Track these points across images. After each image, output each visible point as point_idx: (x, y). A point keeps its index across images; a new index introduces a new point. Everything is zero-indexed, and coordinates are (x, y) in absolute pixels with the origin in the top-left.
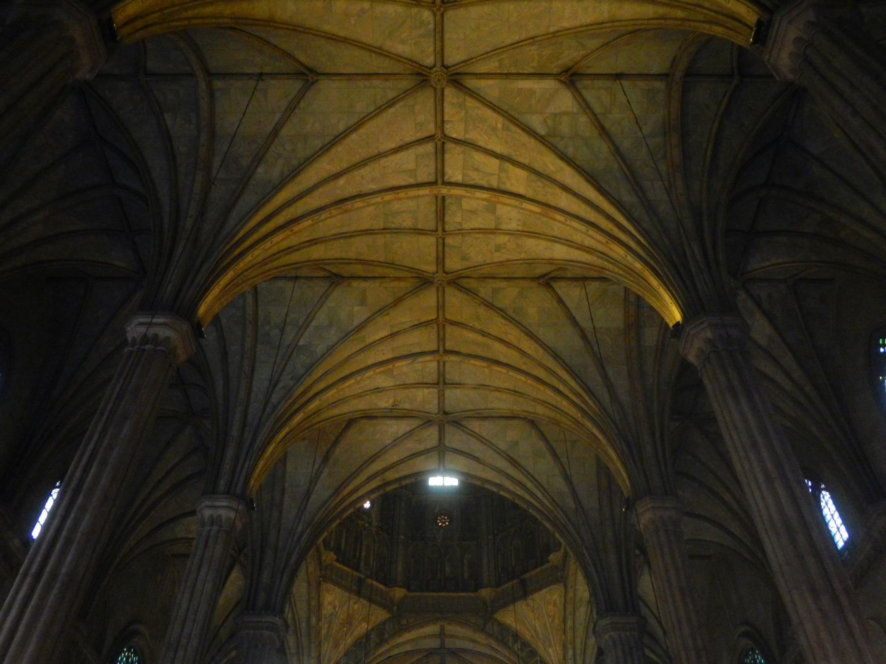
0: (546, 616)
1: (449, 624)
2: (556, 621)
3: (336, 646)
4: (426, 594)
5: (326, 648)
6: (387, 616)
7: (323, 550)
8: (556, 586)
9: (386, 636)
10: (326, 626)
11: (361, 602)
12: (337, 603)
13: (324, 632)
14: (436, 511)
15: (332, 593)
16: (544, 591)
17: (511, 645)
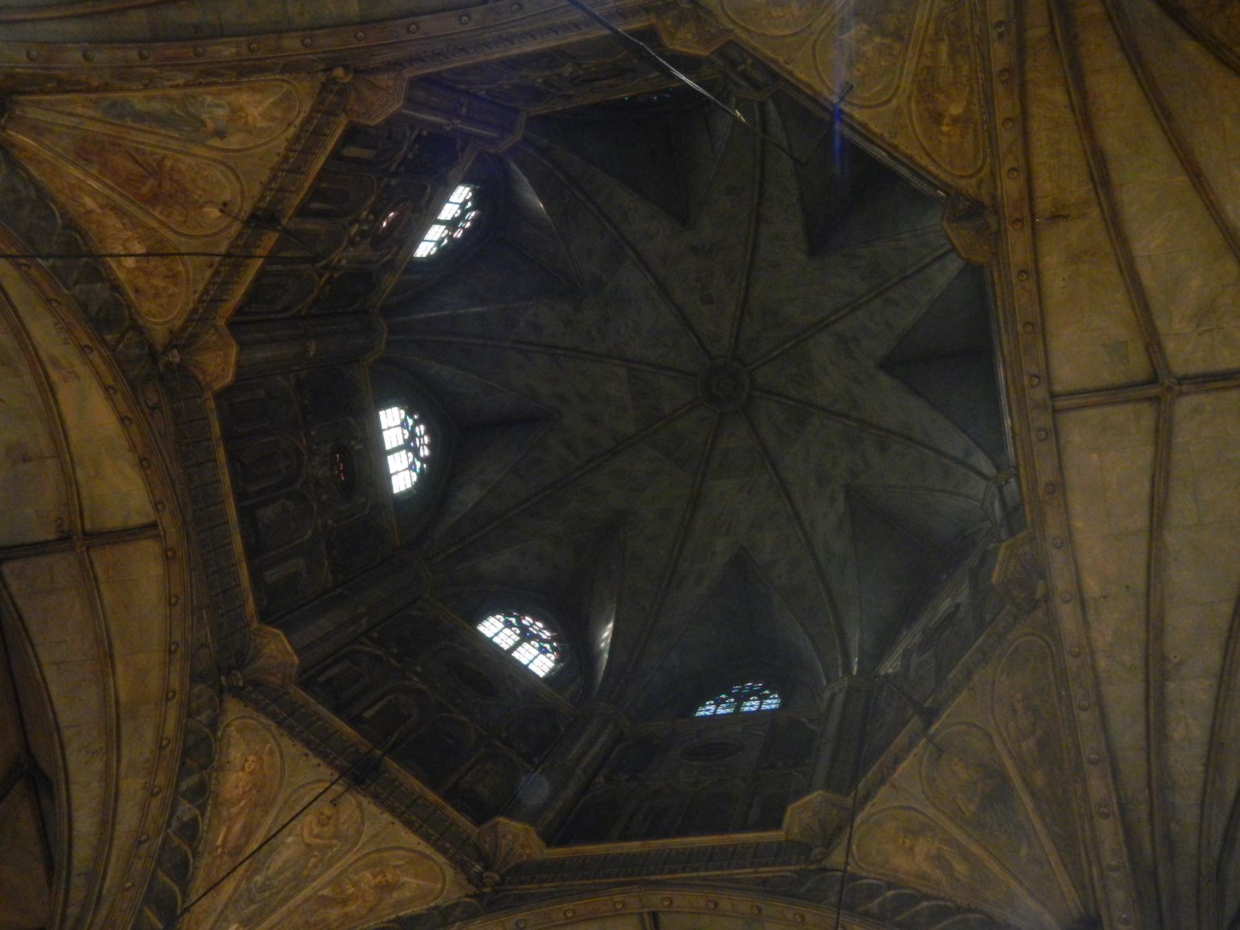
0: (332, 872)
1: (168, 556)
2: (334, 914)
3: (86, 151)
4: (221, 455)
5: (79, 110)
6: (159, 335)
7: (409, 73)
8: (450, 872)
9: (109, 337)
10: (156, 106)
11: (229, 226)
12: (235, 141)
13: (137, 99)
14: (353, 443)
15: (273, 119)
16: (411, 839)
17: (184, 786)
